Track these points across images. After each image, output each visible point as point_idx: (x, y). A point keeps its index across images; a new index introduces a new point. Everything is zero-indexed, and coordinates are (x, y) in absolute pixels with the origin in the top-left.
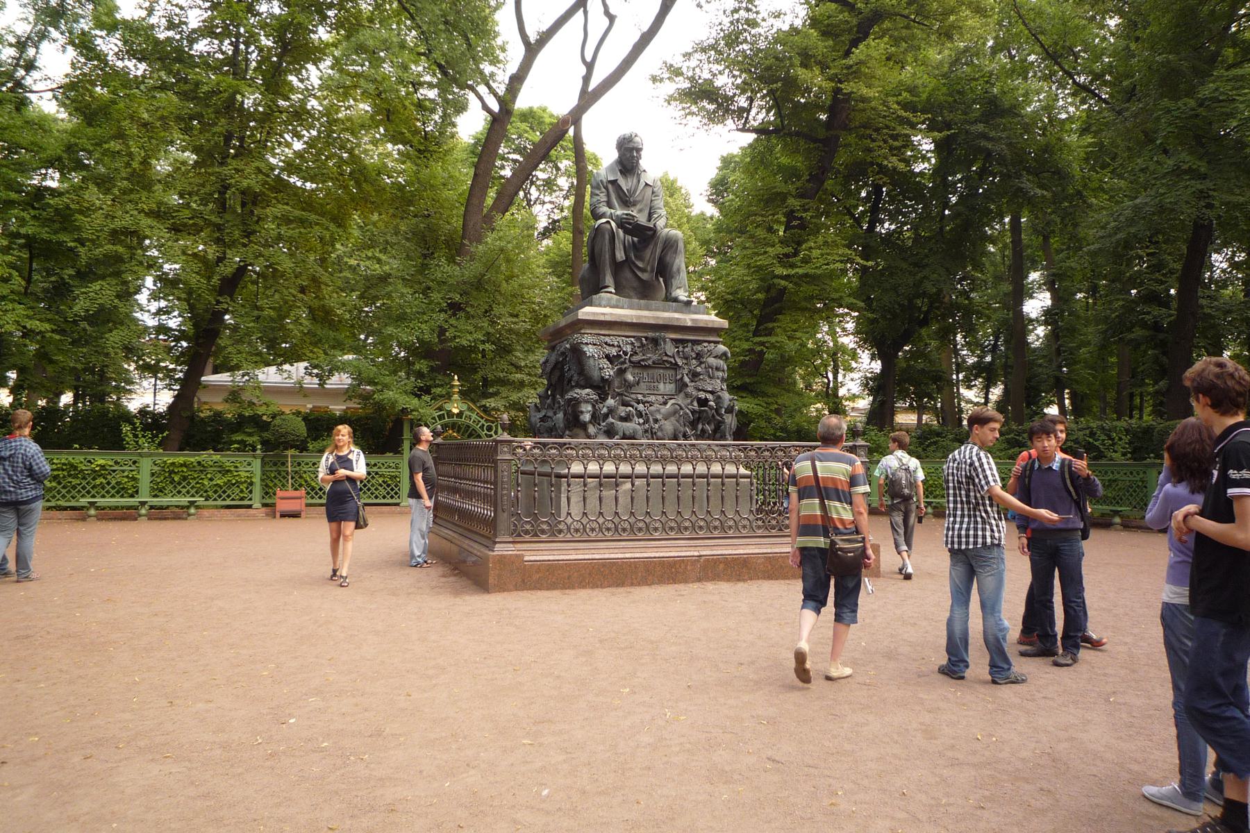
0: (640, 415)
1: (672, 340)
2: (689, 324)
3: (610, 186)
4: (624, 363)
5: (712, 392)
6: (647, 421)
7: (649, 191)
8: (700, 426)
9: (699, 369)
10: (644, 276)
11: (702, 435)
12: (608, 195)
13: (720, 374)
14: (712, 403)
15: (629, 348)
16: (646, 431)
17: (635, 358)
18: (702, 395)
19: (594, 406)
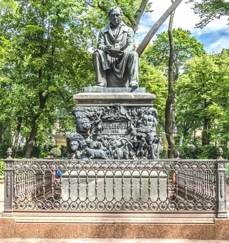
1: (124, 107)
2: (133, 97)
5: (146, 133)
6: (108, 149)
7: (126, 34)
9: (140, 121)
10: (119, 76)
11: (140, 155)
12: (105, 39)
13: (152, 123)
14: (143, 139)
15: (101, 112)
16: (108, 154)
17: (104, 117)
18: (139, 134)
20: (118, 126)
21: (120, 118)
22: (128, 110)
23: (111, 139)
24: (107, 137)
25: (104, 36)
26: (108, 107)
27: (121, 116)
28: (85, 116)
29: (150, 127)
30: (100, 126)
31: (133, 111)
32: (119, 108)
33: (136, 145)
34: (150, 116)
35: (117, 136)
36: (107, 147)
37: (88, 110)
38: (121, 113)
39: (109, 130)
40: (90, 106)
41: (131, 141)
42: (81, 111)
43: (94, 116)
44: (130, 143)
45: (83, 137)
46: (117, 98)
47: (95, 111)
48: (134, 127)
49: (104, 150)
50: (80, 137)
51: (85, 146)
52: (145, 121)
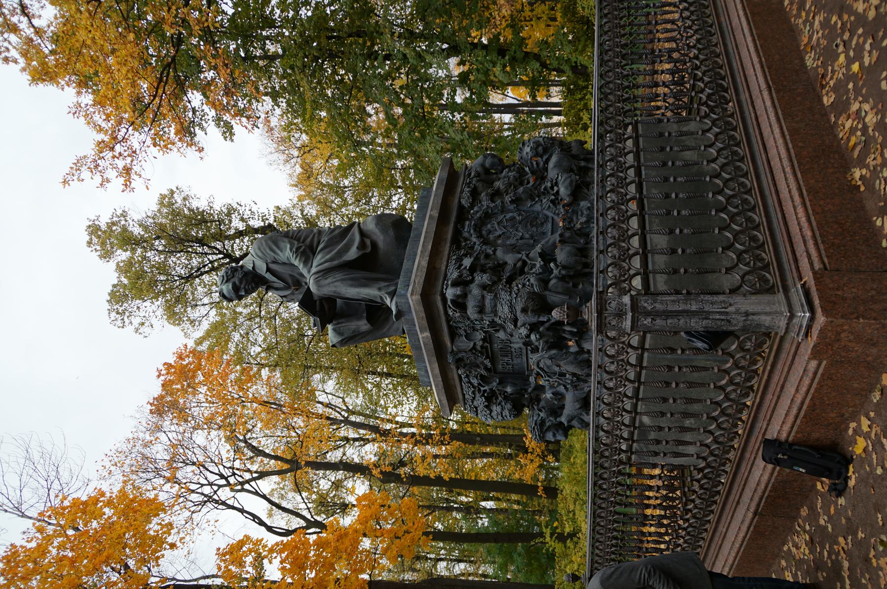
2: (427, 334)
38: (471, 350)
39: (515, 362)
46: (434, 359)
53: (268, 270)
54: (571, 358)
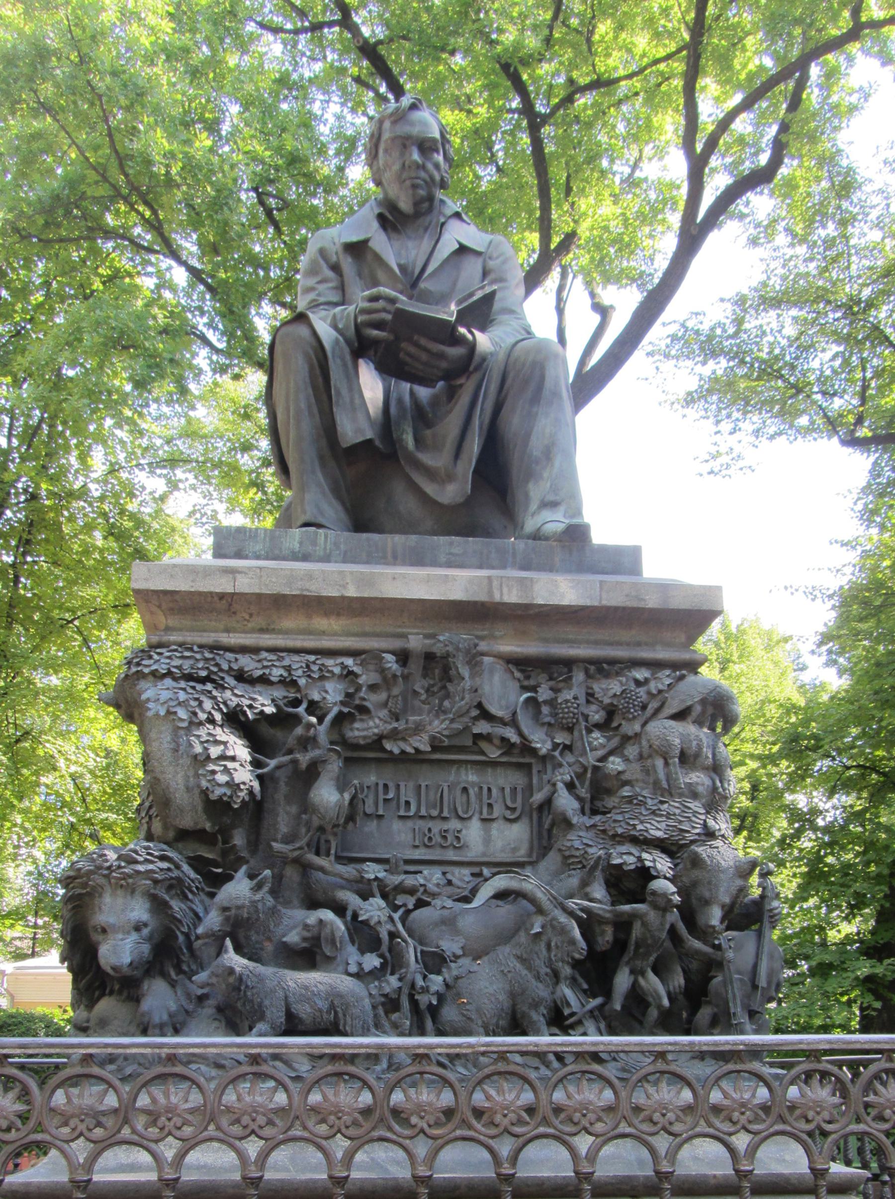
0: (364, 935)
3: (347, 264)
4: (307, 742)
6: (393, 962)
8: (622, 981)
9: (615, 764)
16: (391, 1004)
17: (361, 730)
18: (626, 857)
19: (159, 906)
20: (460, 800)
21: (478, 737)
22: (534, 689)
23: (411, 891)
24: (381, 875)
25: (336, 268)
26: (389, 657)
27: (483, 727)
28: (218, 717)
29: (696, 806)
30: (327, 795)
31: (567, 695)
32: (465, 672)
33: (606, 938)
34: (689, 728)
35: (457, 870)
36: (384, 948)
37: (241, 677)
38: (480, 706)
39: (397, 825)
40: (254, 650)
41: (572, 904)
42: (189, 677)
43: (283, 719)
44: (563, 918)
45: (193, 875)
47: (289, 683)
48: (576, 805)
49: (359, 975)
50: (176, 873)
51: (217, 941)
52: (659, 763)
53: (462, 250)
54: (541, 991)
